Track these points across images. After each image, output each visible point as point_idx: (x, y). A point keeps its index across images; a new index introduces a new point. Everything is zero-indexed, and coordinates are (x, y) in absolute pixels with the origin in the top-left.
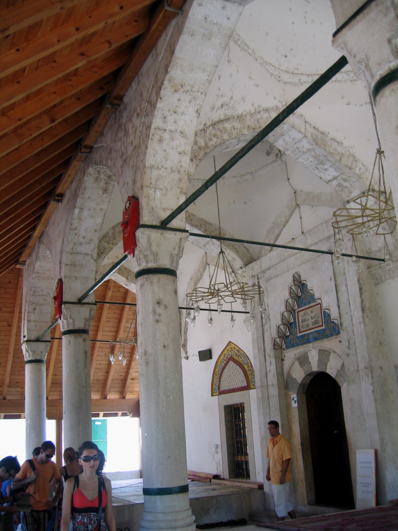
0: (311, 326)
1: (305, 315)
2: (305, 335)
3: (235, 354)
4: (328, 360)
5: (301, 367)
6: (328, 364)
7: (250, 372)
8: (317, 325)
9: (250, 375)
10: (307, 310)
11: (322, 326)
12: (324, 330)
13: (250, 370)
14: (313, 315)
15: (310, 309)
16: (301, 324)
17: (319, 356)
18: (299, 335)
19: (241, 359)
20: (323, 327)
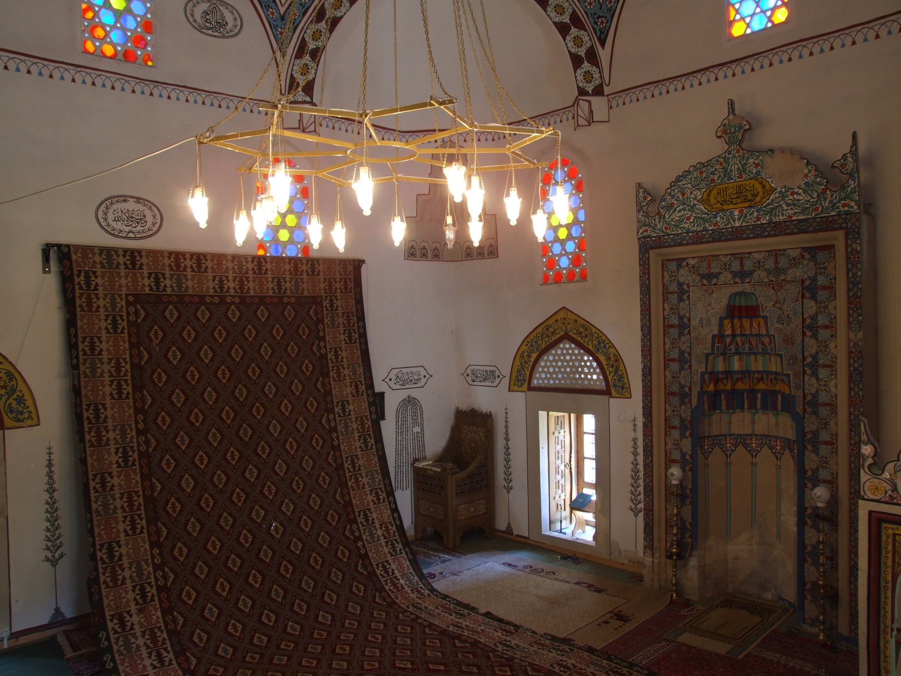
3: (575, 332)
7: (611, 369)
9: (612, 374)
13: (612, 366)
19: (590, 343)
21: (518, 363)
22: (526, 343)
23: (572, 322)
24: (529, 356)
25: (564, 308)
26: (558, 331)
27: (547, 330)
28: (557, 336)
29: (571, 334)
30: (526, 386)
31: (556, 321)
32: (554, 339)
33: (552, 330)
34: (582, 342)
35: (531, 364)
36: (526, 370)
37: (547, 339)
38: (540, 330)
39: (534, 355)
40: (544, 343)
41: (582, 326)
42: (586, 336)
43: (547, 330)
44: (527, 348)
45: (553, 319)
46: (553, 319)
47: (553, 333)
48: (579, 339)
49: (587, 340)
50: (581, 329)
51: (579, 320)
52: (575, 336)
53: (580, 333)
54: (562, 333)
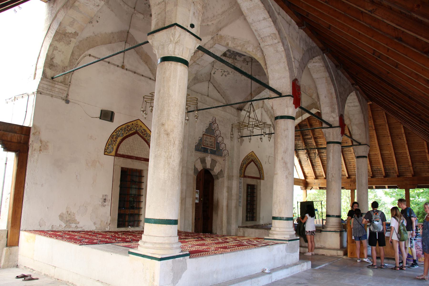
0: (209, 146)
1: (206, 138)
2: (206, 148)
3: (140, 131)
4: (215, 165)
5: (201, 163)
6: (215, 167)
8: (212, 147)
10: (208, 137)
11: (215, 148)
12: (215, 151)
14: (211, 141)
15: (210, 137)
16: (204, 142)
17: (211, 162)
18: (202, 146)
20: (215, 149)
21: (110, 140)
22: (116, 131)
23: (139, 126)
24: (116, 138)
25: (139, 119)
26: (133, 129)
27: (127, 127)
28: (132, 132)
29: (138, 131)
30: (113, 153)
31: (132, 124)
32: (130, 132)
33: (130, 128)
34: (143, 136)
35: (117, 143)
36: (114, 145)
37: (127, 132)
38: (124, 126)
39: (119, 139)
40: (125, 133)
41: (144, 130)
42: (145, 135)
43: (127, 127)
44: (116, 134)
45: (131, 123)
46: (131, 123)
47: (130, 130)
48: (142, 135)
49: (145, 136)
50: (143, 131)
51: (143, 126)
52: (140, 133)
53: (142, 132)
54: (134, 131)
